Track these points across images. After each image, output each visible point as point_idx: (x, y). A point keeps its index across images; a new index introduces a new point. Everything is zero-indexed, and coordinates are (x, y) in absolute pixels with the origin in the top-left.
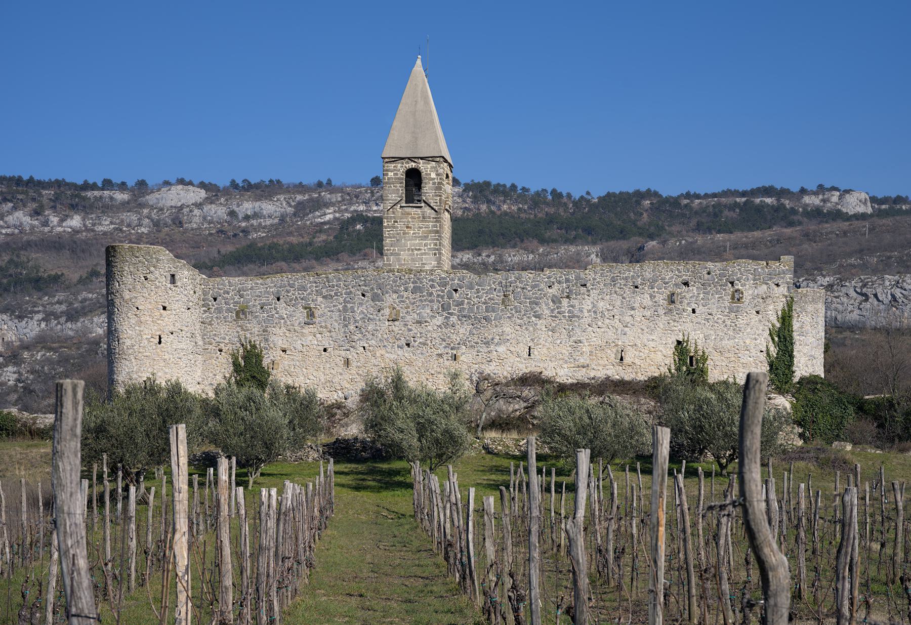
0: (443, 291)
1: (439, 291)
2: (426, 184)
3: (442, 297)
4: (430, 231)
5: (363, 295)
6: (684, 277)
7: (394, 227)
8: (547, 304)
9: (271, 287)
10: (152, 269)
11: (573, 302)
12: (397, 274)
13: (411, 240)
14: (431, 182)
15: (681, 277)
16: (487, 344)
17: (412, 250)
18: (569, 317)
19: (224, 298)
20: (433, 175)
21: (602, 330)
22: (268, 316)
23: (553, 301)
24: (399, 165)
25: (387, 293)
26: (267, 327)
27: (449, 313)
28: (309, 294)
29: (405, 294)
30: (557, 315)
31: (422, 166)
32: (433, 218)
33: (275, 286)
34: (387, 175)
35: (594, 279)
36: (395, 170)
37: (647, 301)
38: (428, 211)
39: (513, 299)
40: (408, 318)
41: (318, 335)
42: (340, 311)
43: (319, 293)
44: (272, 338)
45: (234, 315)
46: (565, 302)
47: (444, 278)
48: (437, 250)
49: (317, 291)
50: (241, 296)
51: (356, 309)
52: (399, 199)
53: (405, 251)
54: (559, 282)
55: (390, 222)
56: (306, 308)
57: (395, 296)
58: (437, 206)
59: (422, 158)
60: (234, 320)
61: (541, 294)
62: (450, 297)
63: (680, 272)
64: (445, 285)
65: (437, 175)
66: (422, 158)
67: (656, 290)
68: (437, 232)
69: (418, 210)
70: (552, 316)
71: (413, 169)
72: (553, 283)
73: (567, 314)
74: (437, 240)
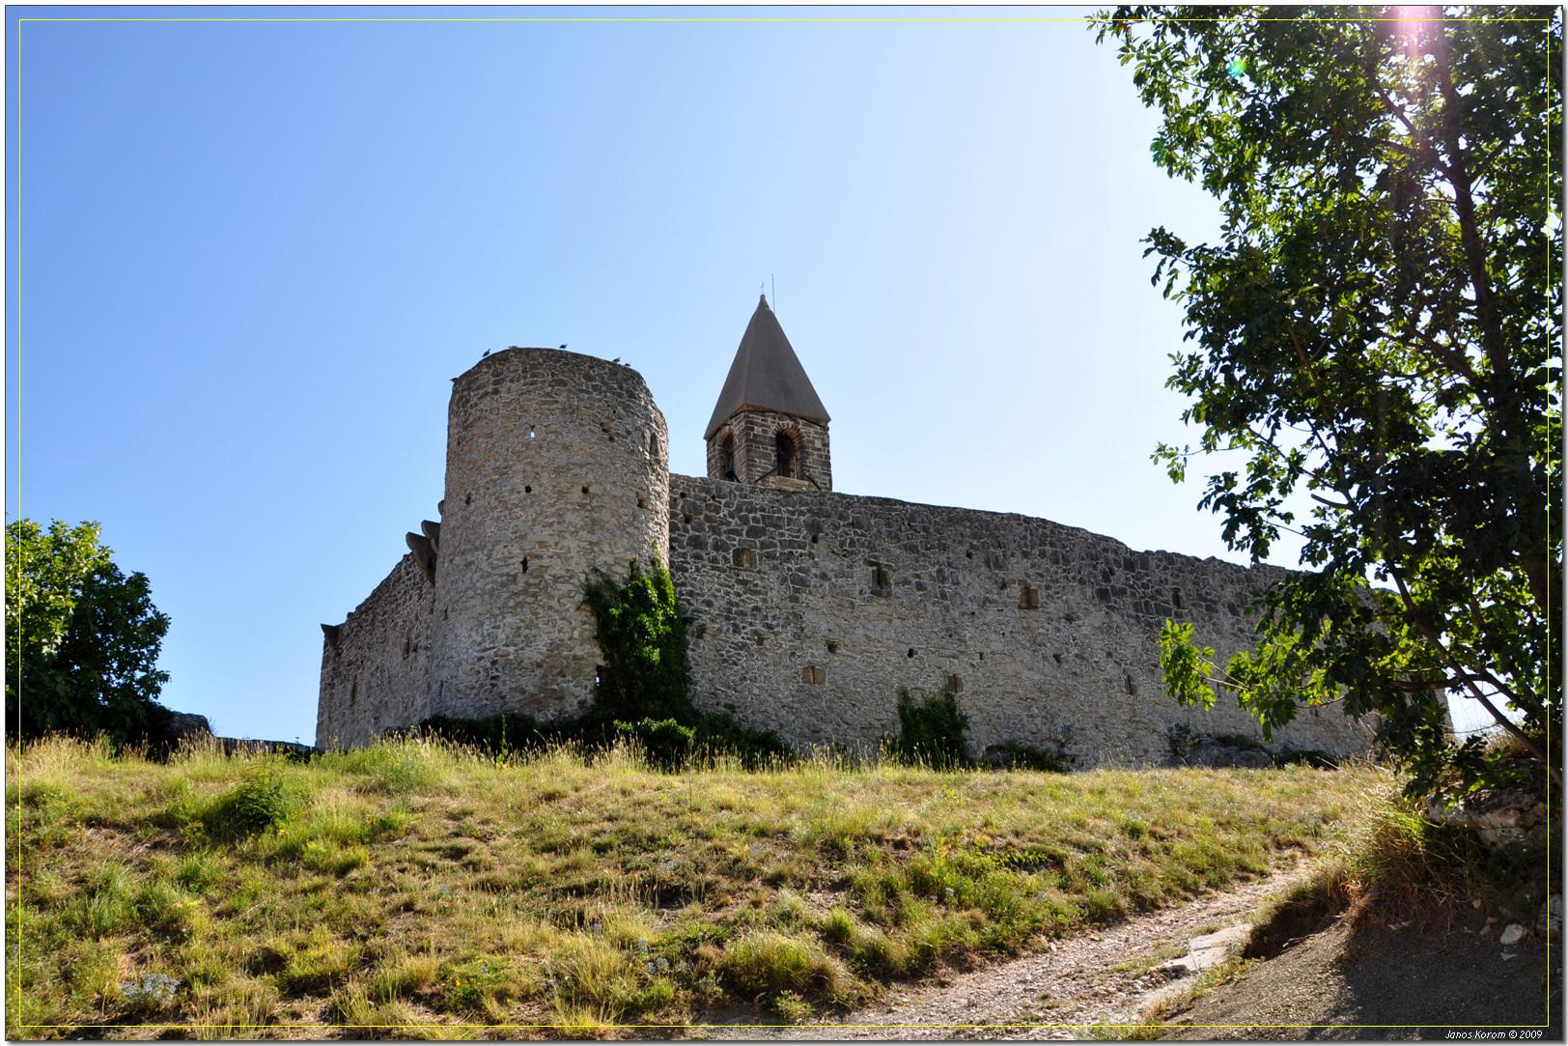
5: (969, 555)
9: (802, 513)
14: (816, 453)
19: (708, 519)
22: (799, 570)
25: (1013, 555)
26: (797, 591)
29: (1045, 563)
33: (809, 511)
34: (753, 429)
41: (897, 622)
45: (730, 556)
50: (745, 521)
51: (960, 579)
56: (871, 564)
59: (802, 418)
60: (730, 568)
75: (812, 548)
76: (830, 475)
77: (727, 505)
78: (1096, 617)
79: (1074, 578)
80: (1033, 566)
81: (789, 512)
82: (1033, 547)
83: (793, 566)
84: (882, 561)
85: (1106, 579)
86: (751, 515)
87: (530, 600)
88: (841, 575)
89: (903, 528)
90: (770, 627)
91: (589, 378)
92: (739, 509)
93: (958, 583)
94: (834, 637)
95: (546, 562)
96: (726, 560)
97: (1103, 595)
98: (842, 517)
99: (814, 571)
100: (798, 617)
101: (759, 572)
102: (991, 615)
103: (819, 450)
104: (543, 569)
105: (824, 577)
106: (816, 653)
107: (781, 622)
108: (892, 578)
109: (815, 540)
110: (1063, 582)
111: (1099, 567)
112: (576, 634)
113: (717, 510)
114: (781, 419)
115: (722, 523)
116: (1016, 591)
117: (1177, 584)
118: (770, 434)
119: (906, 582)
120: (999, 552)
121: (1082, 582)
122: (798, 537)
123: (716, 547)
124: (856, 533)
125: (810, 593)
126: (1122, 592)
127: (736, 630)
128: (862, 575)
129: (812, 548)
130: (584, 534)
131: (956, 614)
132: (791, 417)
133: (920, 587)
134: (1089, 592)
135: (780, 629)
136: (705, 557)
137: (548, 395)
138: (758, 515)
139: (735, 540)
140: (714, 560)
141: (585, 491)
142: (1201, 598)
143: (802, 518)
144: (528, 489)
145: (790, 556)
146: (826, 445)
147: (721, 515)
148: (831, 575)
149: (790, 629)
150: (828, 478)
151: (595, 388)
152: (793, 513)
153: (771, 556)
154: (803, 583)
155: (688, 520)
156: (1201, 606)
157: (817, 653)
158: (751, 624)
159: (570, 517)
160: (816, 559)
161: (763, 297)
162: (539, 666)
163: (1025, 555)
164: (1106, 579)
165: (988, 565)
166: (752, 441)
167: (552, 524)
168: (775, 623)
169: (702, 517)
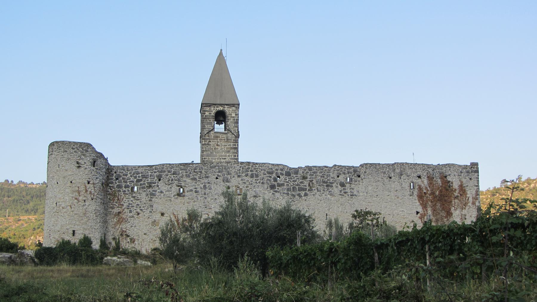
0: (270, 177)
1: (268, 176)
2: (228, 119)
3: (270, 180)
4: (231, 148)
6: (419, 173)
7: (209, 145)
8: (337, 187)
9: (155, 172)
10: (83, 157)
11: (353, 186)
12: (240, 165)
13: (220, 153)
14: (232, 119)
15: (417, 172)
17: (220, 159)
18: (351, 195)
21: (372, 204)
22: (153, 191)
23: (340, 185)
24: (212, 108)
25: (234, 177)
26: (151, 198)
27: (274, 191)
28: (182, 177)
29: (247, 178)
30: (344, 194)
31: (227, 110)
32: (233, 140)
34: (205, 114)
35: (365, 172)
36: (210, 111)
37: (399, 188)
38: (230, 136)
39: (315, 183)
42: (201, 188)
43: (187, 176)
44: (155, 206)
45: (130, 189)
47: (272, 169)
48: (236, 159)
49: (186, 175)
50: (135, 177)
52: (212, 128)
53: (215, 159)
54: (344, 173)
55: (207, 141)
56: (179, 186)
57: (240, 179)
58: (236, 133)
59: (227, 105)
60: (130, 193)
61: (333, 180)
62: (275, 180)
63: (416, 170)
65: (236, 115)
66: (227, 105)
67: (403, 180)
69: (225, 136)
70: (340, 195)
71: (220, 111)
72: (340, 174)
73: (349, 194)
74: (236, 153)
75: (158, 183)
76: (238, 127)
77: (130, 173)
79: (259, 182)
80: (242, 180)
81: (151, 172)
82: (242, 173)
83: (151, 190)
86: (138, 176)
87: (57, 214)
88: (168, 191)
89: (192, 172)
90: (141, 210)
91: (73, 149)
92: (134, 174)
93: (211, 189)
94: (163, 211)
95: (61, 203)
96: (128, 191)
97: (272, 187)
98: (169, 172)
99: (158, 191)
100: (152, 206)
101: (139, 193)
103: (234, 117)
104: (60, 205)
105: (162, 192)
106: (157, 217)
107: (146, 208)
109: (160, 180)
110: (254, 184)
111: (272, 177)
112: (67, 223)
113: (126, 175)
114: (217, 107)
115: (128, 179)
117: (313, 178)
118: (212, 114)
119: (191, 190)
120: (229, 176)
121: (263, 183)
122: (153, 180)
123: (125, 187)
124: (174, 177)
125: (156, 198)
127: (131, 212)
128: (175, 189)
129: (158, 183)
130: (71, 195)
131: (209, 199)
132: (221, 105)
133: (196, 192)
134: (266, 186)
135: (145, 210)
136: (122, 191)
137: (62, 155)
138: (140, 175)
139: (132, 184)
140: (125, 191)
141: (71, 182)
142: (324, 182)
143: (155, 174)
144: (58, 183)
145: (150, 186)
146: (237, 115)
147: (128, 177)
148: (164, 191)
149: (149, 210)
150: (237, 128)
151: (75, 152)
152: (152, 173)
153: (143, 188)
154: (154, 195)
155: (117, 179)
156: (324, 186)
157: (157, 216)
158: (135, 210)
160: (159, 187)
161: (221, 50)
162: (59, 231)
163: (239, 176)
165: (224, 181)
166: (204, 118)
167: (62, 193)
168: (143, 209)
169: (121, 178)
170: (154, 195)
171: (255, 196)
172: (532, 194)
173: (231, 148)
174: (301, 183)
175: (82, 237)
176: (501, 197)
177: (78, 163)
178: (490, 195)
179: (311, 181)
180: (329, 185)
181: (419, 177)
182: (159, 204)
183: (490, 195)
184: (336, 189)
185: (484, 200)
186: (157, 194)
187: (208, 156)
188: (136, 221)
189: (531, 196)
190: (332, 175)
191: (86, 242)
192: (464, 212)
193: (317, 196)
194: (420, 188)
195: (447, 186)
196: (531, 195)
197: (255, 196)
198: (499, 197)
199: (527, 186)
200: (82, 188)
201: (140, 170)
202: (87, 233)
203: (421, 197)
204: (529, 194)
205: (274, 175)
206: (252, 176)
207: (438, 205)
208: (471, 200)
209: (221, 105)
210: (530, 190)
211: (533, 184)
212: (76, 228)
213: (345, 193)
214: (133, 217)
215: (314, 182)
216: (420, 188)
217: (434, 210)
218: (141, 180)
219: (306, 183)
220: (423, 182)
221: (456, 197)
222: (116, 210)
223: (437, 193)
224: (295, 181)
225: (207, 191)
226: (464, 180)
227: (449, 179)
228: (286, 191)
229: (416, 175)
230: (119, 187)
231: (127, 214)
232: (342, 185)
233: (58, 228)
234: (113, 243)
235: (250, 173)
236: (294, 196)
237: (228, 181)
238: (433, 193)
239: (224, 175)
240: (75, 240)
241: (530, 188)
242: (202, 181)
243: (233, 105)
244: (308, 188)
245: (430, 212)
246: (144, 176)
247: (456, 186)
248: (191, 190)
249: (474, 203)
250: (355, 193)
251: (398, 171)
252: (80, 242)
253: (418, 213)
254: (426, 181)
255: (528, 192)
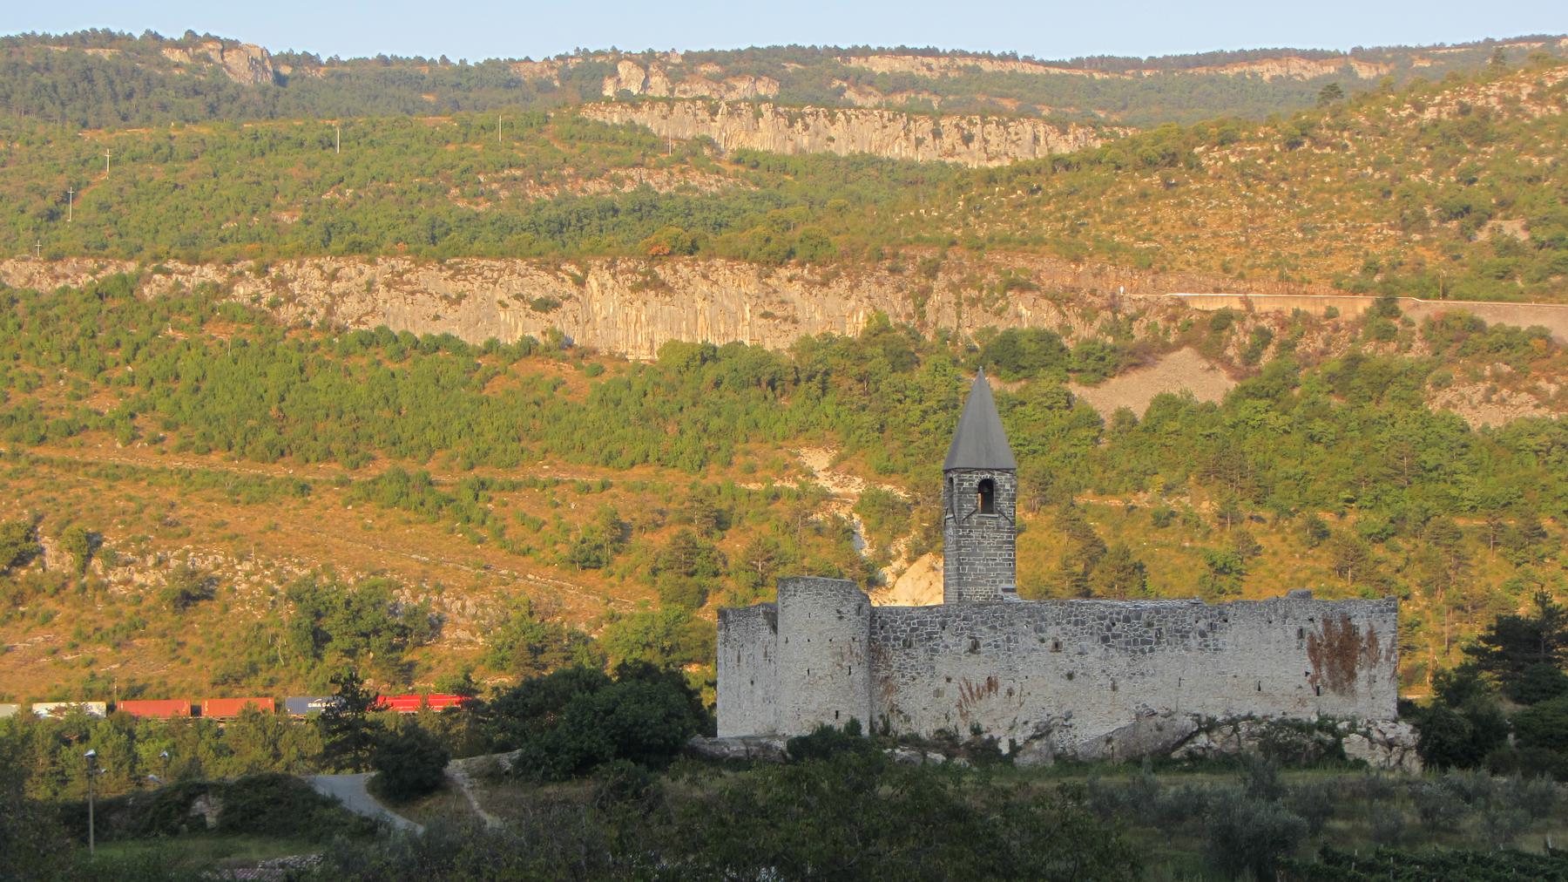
16: (1142, 674)
20: (1007, 487)
28: (976, 624)
29: (1069, 627)
31: (997, 477)
37: (1282, 637)
38: (1002, 521)
40: (1070, 650)
43: (984, 623)
46: (1210, 634)
50: (909, 625)
57: (1059, 628)
64: (1104, 618)
68: (1010, 542)
69: (994, 522)
78: (1099, 650)
83: (931, 643)
84: (977, 636)
85: (1109, 629)
88: (956, 645)
94: (949, 675)
97: (1105, 639)
98: (957, 616)
100: (933, 668)
102: (1034, 657)
108: (982, 643)
116: (1050, 643)
119: (990, 645)
123: (895, 639)
126: (1120, 636)
127: (903, 676)
128: (966, 643)
132: (989, 470)
133: (996, 646)
134: (1096, 638)
142: (1177, 631)
145: (931, 638)
149: (930, 673)
153: (921, 641)
154: (937, 651)
155: (882, 628)
157: (941, 683)
159: (825, 652)
163: (1058, 624)
164: (1109, 629)
170: (937, 651)
171: (1080, 654)
172: (1430, 148)
173: (1005, 542)
174: (1146, 632)
175: (848, 719)
176: (1317, 151)
177: (839, 612)
178: (1278, 141)
179: (1159, 630)
180: (1185, 636)
181: (1311, 620)
182: (943, 665)
183: (1278, 141)
184: (1194, 642)
185: (1260, 161)
186: (941, 649)
187: (967, 555)
188: (912, 691)
189: (1424, 156)
190: (1188, 621)
191: (854, 726)
192: (1374, 671)
193: (1167, 651)
194: (1312, 638)
195: (1350, 633)
196: (1424, 149)
197: (1080, 654)
198: (1313, 154)
199: (1411, 116)
200: (846, 649)
201: (915, 614)
202: (854, 714)
203: (1313, 651)
204: (1418, 146)
205: (1107, 622)
206: (1076, 623)
207: (1337, 661)
208: (1384, 653)
209: (989, 470)
210: (1423, 130)
211: (1431, 109)
212: (840, 707)
213: (1207, 646)
214: (906, 683)
215: (1163, 630)
216: (1312, 638)
217: (1331, 671)
218: (917, 629)
219: (1152, 633)
220: (1316, 627)
221: (1364, 650)
222: (882, 674)
223: (1336, 644)
224: (1136, 630)
225: (1012, 645)
226: (1375, 624)
227: (1354, 622)
228: (1123, 646)
229: (1306, 617)
230: (886, 639)
231: (898, 679)
232: (1203, 634)
233: (813, 707)
234: (881, 723)
235: (1073, 618)
236: (1135, 652)
237: (1042, 630)
238: (1330, 645)
239: (1036, 621)
240: (840, 725)
241: (1420, 124)
242: (1005, 630)
243: (1007, 471)
244: (1154, 640)
245: (1324, 672)
246: (920, 623)
247: (1363, 632)
248: (990, 645)
249: (1388, 659)
250: (1220, 646)
251: (1281, 612)
252: (847, 728)
253: (1307, 674)
254: (1320, 627)
255: (1415, 140)
